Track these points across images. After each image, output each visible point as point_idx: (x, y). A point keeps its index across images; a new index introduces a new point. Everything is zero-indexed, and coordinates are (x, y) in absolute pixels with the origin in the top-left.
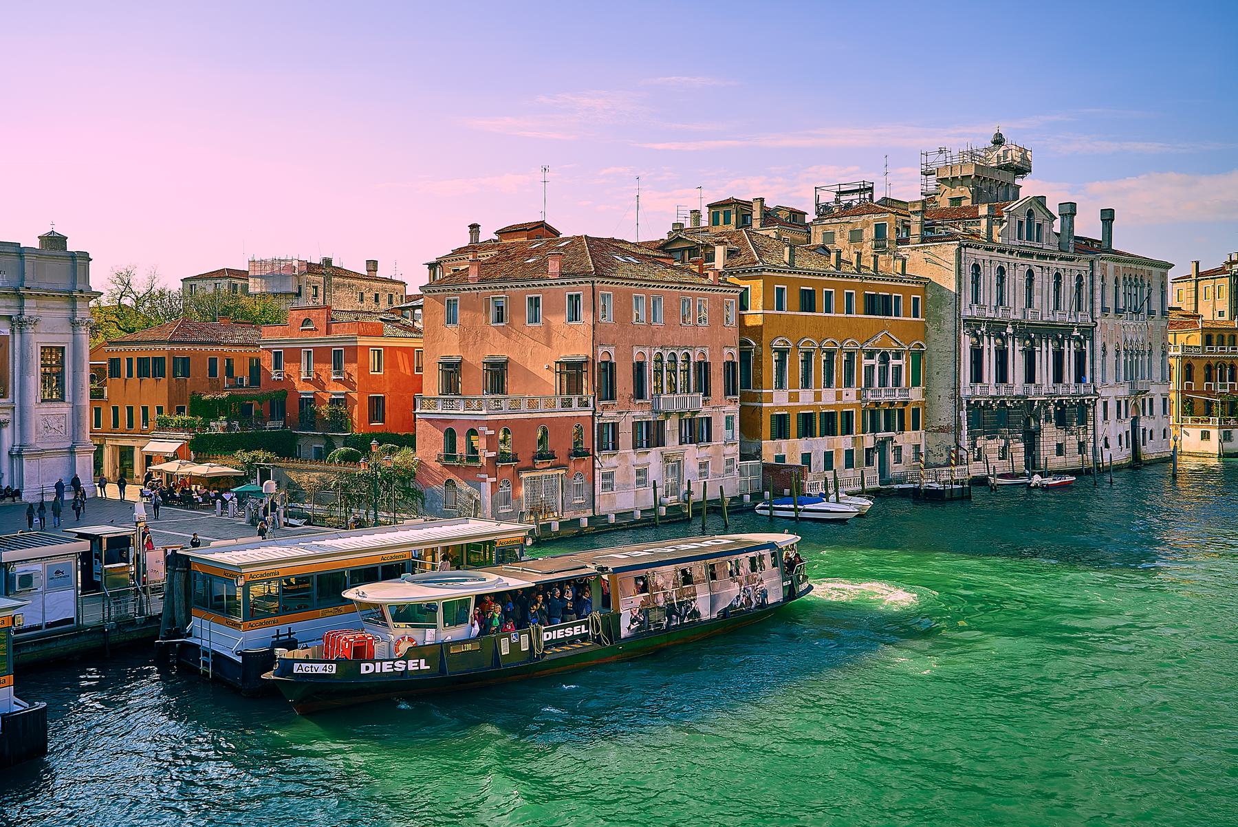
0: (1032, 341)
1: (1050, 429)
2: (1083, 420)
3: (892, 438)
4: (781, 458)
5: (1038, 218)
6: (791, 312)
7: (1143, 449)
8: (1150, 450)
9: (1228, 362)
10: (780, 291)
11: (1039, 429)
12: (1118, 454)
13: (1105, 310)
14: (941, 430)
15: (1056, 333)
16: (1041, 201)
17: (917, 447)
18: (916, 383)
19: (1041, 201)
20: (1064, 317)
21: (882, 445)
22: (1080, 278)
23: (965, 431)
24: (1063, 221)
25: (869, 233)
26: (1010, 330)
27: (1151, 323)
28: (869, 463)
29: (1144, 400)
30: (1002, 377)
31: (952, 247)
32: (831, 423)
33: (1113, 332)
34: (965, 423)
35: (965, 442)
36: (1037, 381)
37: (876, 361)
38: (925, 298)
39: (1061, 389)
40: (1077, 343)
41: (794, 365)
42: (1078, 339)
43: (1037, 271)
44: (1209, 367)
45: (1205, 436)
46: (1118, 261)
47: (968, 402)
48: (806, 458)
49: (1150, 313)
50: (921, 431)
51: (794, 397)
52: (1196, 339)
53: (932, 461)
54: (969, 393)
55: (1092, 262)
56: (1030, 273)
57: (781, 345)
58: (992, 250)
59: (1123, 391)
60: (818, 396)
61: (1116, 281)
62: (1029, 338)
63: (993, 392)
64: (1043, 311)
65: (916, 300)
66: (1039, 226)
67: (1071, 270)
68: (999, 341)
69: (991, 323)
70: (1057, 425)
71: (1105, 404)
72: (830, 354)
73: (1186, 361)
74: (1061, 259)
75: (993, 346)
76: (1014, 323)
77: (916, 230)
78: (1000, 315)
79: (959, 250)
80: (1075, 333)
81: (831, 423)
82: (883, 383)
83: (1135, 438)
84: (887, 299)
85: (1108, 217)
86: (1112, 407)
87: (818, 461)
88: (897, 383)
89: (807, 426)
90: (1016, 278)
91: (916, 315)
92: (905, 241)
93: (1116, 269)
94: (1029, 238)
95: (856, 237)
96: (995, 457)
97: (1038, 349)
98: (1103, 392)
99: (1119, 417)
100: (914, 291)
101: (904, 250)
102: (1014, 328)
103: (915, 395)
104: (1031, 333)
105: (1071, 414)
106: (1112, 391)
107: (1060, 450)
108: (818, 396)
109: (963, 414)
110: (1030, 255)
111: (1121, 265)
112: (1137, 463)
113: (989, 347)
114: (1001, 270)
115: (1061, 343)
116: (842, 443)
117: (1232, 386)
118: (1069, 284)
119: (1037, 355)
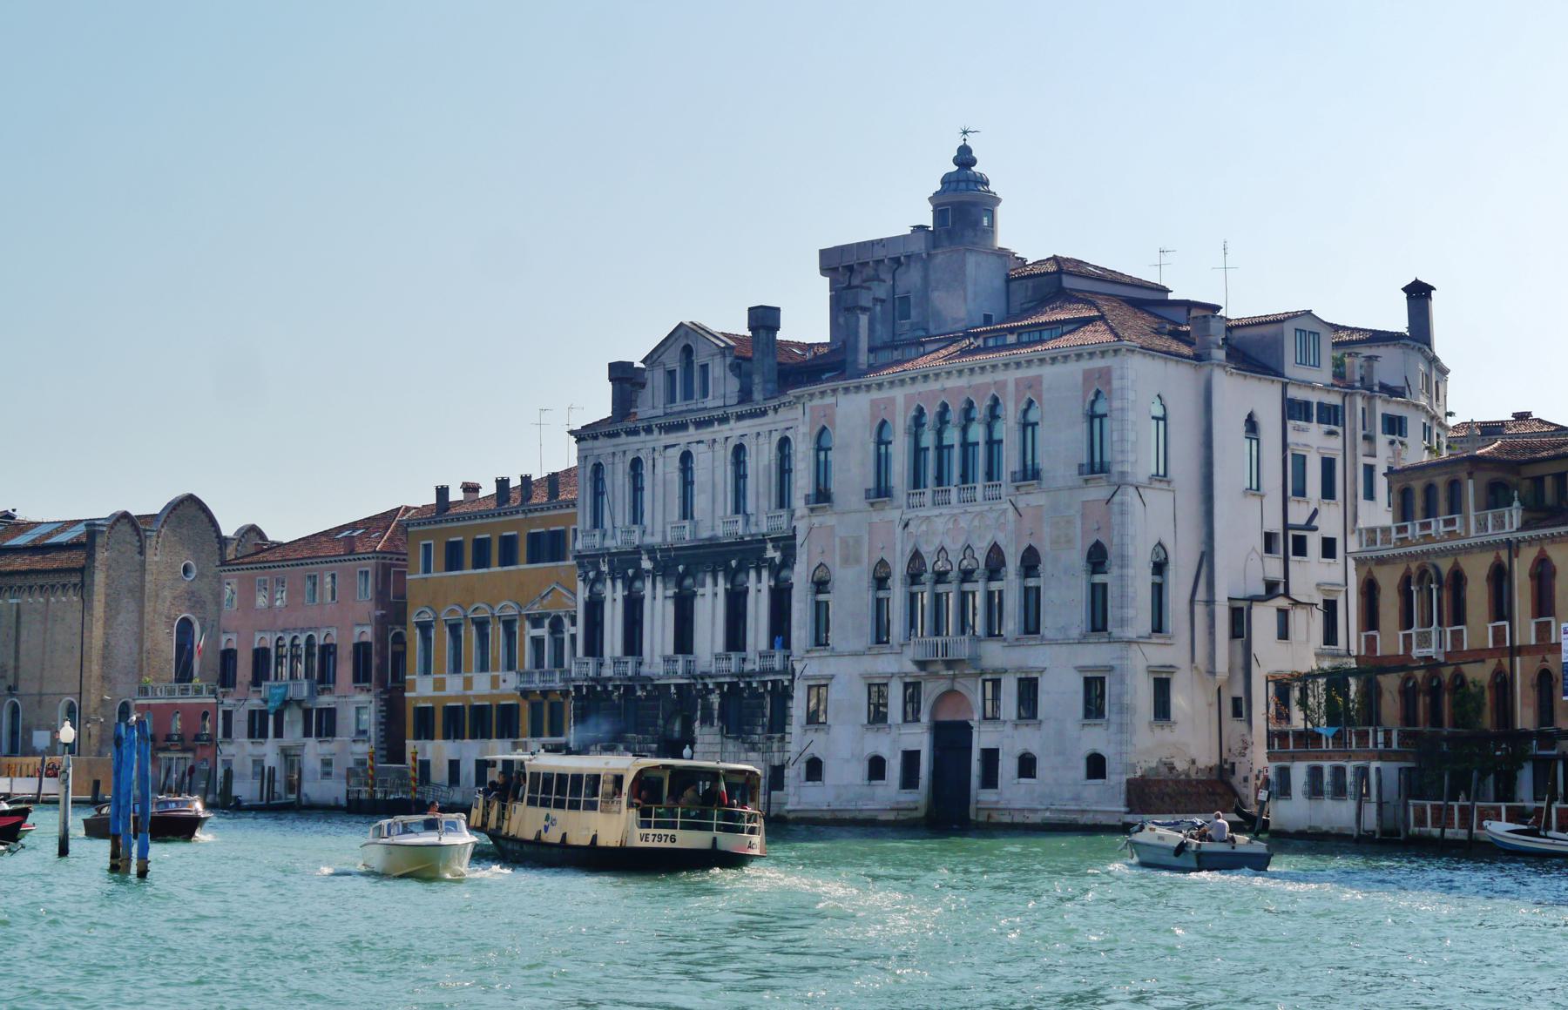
1: (708, 739)
9: (1445, 566)
37: (543, 632)
64: (713, 519)
76: (651, 551)
110: (683, 427)
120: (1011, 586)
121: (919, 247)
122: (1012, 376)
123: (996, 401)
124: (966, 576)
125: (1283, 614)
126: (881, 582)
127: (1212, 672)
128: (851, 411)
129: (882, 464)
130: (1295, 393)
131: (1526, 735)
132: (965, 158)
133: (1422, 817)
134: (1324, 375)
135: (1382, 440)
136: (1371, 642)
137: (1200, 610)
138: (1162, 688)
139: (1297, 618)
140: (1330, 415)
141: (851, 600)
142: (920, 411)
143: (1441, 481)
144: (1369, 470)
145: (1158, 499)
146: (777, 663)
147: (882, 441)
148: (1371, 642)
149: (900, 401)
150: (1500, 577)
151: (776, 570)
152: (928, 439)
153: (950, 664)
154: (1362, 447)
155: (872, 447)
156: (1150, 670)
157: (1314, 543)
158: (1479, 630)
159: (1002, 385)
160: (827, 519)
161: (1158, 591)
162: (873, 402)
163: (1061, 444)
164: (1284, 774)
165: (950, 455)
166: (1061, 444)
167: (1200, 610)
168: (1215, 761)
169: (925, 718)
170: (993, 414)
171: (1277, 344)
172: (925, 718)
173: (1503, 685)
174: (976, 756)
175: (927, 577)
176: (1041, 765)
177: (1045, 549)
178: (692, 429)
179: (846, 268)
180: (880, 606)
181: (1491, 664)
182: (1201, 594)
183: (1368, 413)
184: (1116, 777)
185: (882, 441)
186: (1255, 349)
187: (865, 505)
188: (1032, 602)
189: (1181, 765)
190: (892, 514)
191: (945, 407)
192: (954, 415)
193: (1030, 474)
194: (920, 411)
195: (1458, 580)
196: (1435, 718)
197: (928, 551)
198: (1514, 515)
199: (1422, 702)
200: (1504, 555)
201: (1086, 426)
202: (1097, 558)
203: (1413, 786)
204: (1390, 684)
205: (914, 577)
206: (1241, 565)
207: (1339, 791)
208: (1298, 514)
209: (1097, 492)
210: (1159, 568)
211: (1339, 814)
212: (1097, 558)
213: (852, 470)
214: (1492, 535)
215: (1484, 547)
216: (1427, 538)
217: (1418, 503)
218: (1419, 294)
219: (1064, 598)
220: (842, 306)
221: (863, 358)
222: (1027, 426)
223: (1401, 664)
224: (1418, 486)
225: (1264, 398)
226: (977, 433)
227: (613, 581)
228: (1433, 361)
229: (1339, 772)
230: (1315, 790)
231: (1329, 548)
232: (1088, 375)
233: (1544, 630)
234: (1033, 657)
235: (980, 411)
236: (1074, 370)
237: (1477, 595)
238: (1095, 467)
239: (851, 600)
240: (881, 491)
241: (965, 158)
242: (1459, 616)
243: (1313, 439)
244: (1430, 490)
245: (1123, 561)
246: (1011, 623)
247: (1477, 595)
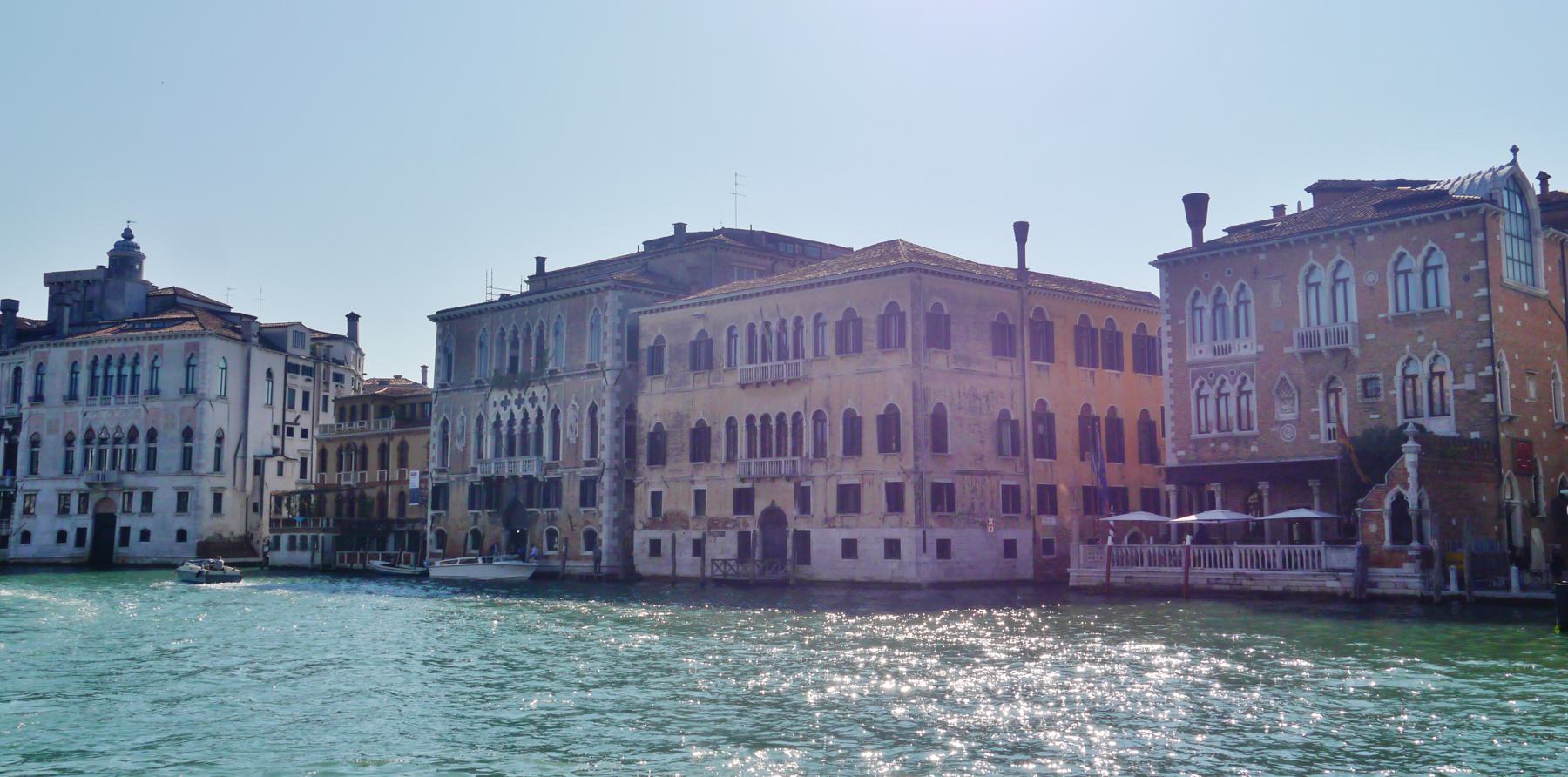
9: (359, 443)
120: (141, 447)
121: (100, 276)
122: (147, 344)
123: (138, 355)
124: (117, 441)
125: (281, 464)
126: (69, 441)
127: (244, 490)
128: (58, 357)
129: (73, 383)
130: (290, 360)
131: (392, 521)
132: (128, 235)
133: (342, 559)
134: (306, 353)
135: (332, 385)
136: (322, 478)
137: (239, 461)
138: (218, 498)
139: (287, 466)
140: (308, 372)
141: (51, 450)
142: (96, 358)
143: (359, 406)
144: (326, 398)
145: (220, 407)
146: (7, 482)
147: (74, 371)
148: (322, 478)
149: (85, 353)
150: (384, 450)
151: (9, 435)
152: (100, 372)
153: (105, 485)
154: (322, 387)
155: (68, 374)
156: (213, 489)
157: (297, 431)
158: (373, 474)
159: (141, 348)
160: (40, 410)
161: (218, 452)
162: (70, 353)
163: (171, 378)
164: (277, 539)
165: (108, 381)
166: (171, 378)
167: (239, 461)
168: (242, 533)
169: (90, 511)
170: (136, 361)
171: (284, 336)
172: (90, 511)
173: (383, 498)
174: (117, 530)
175: (95, 441)
176: (153, 536)
177: (160, 429)
179: (59, 284)
180: (68, 457)
181: (377, 489)
182: (240, 453)
183: (326, 373)
184: (192, 541)
185: (74, 371)
186: (273, 339)
187: (62, 403)
188: (152, 455)
189: (226, 535)
190: (78, 409)
191: (110, 357)
192: (115, 361)
193: (154, 392)
194: (96, 358)
195: (364, 450)
196: (351, 511)
197: (96, 428)
198: (392, 421)
199: (345, 505)
201: (183, 371)
202: (188, 434)
203: (339, 544)
204: (330, 497)
205: (88, 439)
206: (260, 439)
207: (304, 547)
208: (290, 417)
209: (189, 402)
210: (220, 440)
211: (303, 557)
212: (188, 434)
213: (56, 386)
214: (381, 430)
215: (378, 435)
216: (351, 431)
217: (348, 413)
218: (353, 318)
219: (169, 454)
220: (55, 303)
221: (66, 329)
222: (154, 368)
223: (336, 488)
224: (348, 407)
225: (277, 362)
226: (127, 370)
228: (358, 350)
229: (304, 538)
230: (292, 546)
231: (304, 433)
232: (187, 346)
233: (402, 474)
234: (151, 482)
235: (129, 359)
236: (182, 342)
237: (373, 457)
238: (189, 390)
239: (51, 450)
240: (72, 397)
241: (128, 235)
242: (364, 467)
243: (299, 383)
244: (353, 409)
245: (201, 436)
246: (140, 465)
247: (373, 457)
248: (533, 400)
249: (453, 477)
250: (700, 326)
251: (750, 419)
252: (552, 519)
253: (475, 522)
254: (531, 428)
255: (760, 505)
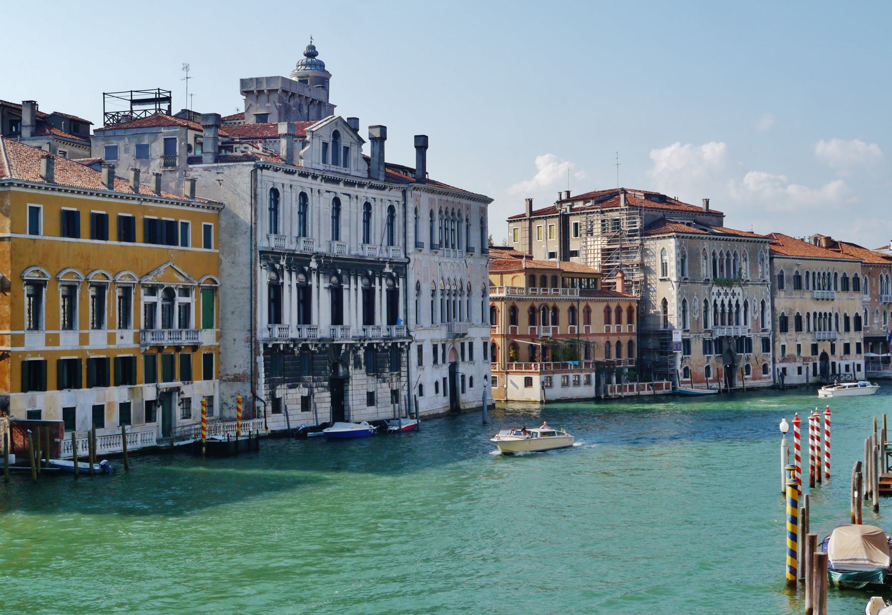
0: (340, 278)
1: (359, 377)
2: (396, 366)
3: (178, 389)
4: (35, 414)
5: (346, 139)
6: (49, 235)
7: (463, 397)
8: (470, 398)
9: (551, 305)
10: (34, 212)
11: (347, 378)
12: (433, 402)
13: (418, 245)
14: (237, 378)
15: (365, 269)
16: (353, 125)
17: (210, 399)
18: (208, 325)
19: (353, 125)
20: (377, 250)
21: (165, 398)
22: (391, 209)
23: (262, 379)
24: (373, 146)
25: (157, 149)
26: (313, 265)
27: (470, 261)
28: (150, 418)
29: (463, 345)
30: (305, 316)
31: (247, 168)
32: (100, 372)
33: (429, 270)
34: (261, 370)
35: (263, 391)
36: (346, 322)
37: (158, 298)
38: (218, 226)
39: (371, 332)
40: (390, 282)
41: (53, 300)
42: (390, 276)
43: (344, 200)
44: (533, 310)
45: (528, 382)
46: (432, 192)
47: (265, 346)
48: (69, 414)
49: (469, 250)
50: (215, 381)
51: (53, 340)
52: (521, 281)
53: (227, 414)
54: (266, 335)
55: (404, 192)
56: (337, 202)
57: (36, 277)
58: (292, 173)
59: (440, 334)
60: (84, 339)
61: (431, 214)
62: (336, 274)
63: (294, 334)
64: (351, 244)
65: (207, 229)
66: (347, 149)
67: (382, 199)
68: (301, 277)
69: (291, 255)
70: (367, 372)
71: (420, 349)
72: (101, 289)
73: (510, 303)
74: (371, 187)
75: (295, 282)
76: (318, 256)
77: (209, 147)
78: (299, 247)
79: (254, 173)
80: (387, 270)
81: (100, 372)
82: (168, 323)
83: (453, 385)
84: (172, 225)
85: (421, 144)
86: (428, 351)
87: (84, 417)
88: (185, 322)
89: (71, 374)
90: (320, 207)
91: (207, 245)
92: (197, 160)
93: (431, 201)
94: (335, 162)
95: (142, 152)
96: (298, 407)
97: (345, 286)
98: (417, 335)
99: (435, 361)
100: (205, 217)
101: (196, 170)
102: (318, 262)
103: (207, 338)
104: (339, 269)
105: (385, 359)
106: (427, 333)
107: (371, 399)
108: (84, 339)
109: (261, 359)
110: (336, 181)
111: (436, 197)
112: (455, 412)
113: (290, 284)
114: (303, 196)
115: (372, 280)
116: (115, 395)
117: (555, 330)
118: (379, 215)
119: (345, 294)
132: (311, 53)
158: (564, 327)
178: (341, 184)
200: (575, 304)
207: (577, 383)
214: (569, 296)
227: (290, 272)
233: (587, 329)
237: (564, 316)
241: (311, 53)
242: (555, 321)
247: (564, 316)
248: (734, 294)
249: (692, 336)
250: (796, 269)
251: (815, 314)
252: (748, 359)
253: (708, 361)
254: (734, 309)
255: (820, 351)
